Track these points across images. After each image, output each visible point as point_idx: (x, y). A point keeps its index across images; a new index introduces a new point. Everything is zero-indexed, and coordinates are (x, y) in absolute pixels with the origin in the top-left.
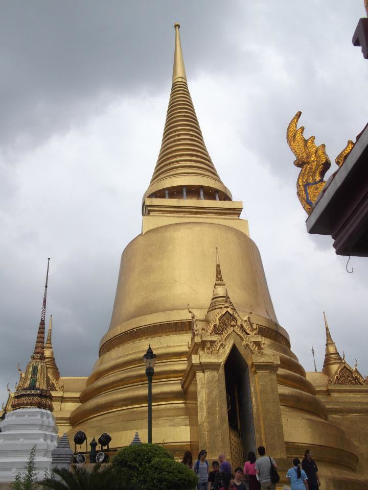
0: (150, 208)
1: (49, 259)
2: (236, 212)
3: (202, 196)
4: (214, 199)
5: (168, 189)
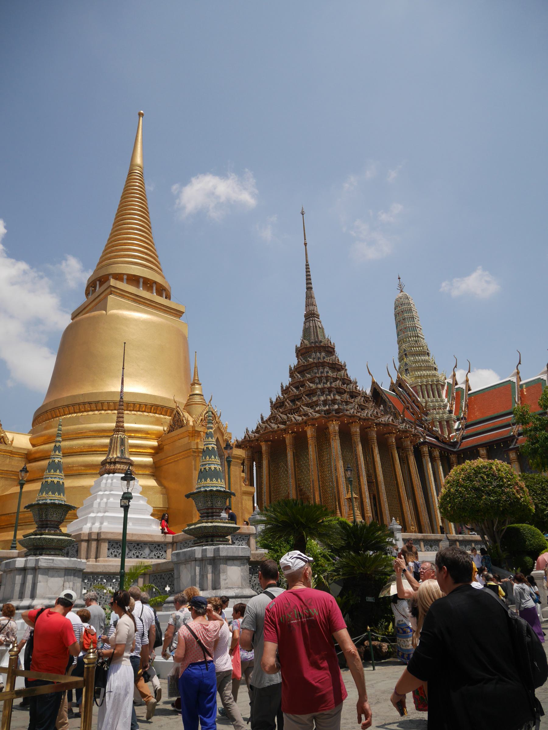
0: (113, 289)
1: (125, 343)
2: (178, 313)
3: (154, 291)
5: (128, 275)
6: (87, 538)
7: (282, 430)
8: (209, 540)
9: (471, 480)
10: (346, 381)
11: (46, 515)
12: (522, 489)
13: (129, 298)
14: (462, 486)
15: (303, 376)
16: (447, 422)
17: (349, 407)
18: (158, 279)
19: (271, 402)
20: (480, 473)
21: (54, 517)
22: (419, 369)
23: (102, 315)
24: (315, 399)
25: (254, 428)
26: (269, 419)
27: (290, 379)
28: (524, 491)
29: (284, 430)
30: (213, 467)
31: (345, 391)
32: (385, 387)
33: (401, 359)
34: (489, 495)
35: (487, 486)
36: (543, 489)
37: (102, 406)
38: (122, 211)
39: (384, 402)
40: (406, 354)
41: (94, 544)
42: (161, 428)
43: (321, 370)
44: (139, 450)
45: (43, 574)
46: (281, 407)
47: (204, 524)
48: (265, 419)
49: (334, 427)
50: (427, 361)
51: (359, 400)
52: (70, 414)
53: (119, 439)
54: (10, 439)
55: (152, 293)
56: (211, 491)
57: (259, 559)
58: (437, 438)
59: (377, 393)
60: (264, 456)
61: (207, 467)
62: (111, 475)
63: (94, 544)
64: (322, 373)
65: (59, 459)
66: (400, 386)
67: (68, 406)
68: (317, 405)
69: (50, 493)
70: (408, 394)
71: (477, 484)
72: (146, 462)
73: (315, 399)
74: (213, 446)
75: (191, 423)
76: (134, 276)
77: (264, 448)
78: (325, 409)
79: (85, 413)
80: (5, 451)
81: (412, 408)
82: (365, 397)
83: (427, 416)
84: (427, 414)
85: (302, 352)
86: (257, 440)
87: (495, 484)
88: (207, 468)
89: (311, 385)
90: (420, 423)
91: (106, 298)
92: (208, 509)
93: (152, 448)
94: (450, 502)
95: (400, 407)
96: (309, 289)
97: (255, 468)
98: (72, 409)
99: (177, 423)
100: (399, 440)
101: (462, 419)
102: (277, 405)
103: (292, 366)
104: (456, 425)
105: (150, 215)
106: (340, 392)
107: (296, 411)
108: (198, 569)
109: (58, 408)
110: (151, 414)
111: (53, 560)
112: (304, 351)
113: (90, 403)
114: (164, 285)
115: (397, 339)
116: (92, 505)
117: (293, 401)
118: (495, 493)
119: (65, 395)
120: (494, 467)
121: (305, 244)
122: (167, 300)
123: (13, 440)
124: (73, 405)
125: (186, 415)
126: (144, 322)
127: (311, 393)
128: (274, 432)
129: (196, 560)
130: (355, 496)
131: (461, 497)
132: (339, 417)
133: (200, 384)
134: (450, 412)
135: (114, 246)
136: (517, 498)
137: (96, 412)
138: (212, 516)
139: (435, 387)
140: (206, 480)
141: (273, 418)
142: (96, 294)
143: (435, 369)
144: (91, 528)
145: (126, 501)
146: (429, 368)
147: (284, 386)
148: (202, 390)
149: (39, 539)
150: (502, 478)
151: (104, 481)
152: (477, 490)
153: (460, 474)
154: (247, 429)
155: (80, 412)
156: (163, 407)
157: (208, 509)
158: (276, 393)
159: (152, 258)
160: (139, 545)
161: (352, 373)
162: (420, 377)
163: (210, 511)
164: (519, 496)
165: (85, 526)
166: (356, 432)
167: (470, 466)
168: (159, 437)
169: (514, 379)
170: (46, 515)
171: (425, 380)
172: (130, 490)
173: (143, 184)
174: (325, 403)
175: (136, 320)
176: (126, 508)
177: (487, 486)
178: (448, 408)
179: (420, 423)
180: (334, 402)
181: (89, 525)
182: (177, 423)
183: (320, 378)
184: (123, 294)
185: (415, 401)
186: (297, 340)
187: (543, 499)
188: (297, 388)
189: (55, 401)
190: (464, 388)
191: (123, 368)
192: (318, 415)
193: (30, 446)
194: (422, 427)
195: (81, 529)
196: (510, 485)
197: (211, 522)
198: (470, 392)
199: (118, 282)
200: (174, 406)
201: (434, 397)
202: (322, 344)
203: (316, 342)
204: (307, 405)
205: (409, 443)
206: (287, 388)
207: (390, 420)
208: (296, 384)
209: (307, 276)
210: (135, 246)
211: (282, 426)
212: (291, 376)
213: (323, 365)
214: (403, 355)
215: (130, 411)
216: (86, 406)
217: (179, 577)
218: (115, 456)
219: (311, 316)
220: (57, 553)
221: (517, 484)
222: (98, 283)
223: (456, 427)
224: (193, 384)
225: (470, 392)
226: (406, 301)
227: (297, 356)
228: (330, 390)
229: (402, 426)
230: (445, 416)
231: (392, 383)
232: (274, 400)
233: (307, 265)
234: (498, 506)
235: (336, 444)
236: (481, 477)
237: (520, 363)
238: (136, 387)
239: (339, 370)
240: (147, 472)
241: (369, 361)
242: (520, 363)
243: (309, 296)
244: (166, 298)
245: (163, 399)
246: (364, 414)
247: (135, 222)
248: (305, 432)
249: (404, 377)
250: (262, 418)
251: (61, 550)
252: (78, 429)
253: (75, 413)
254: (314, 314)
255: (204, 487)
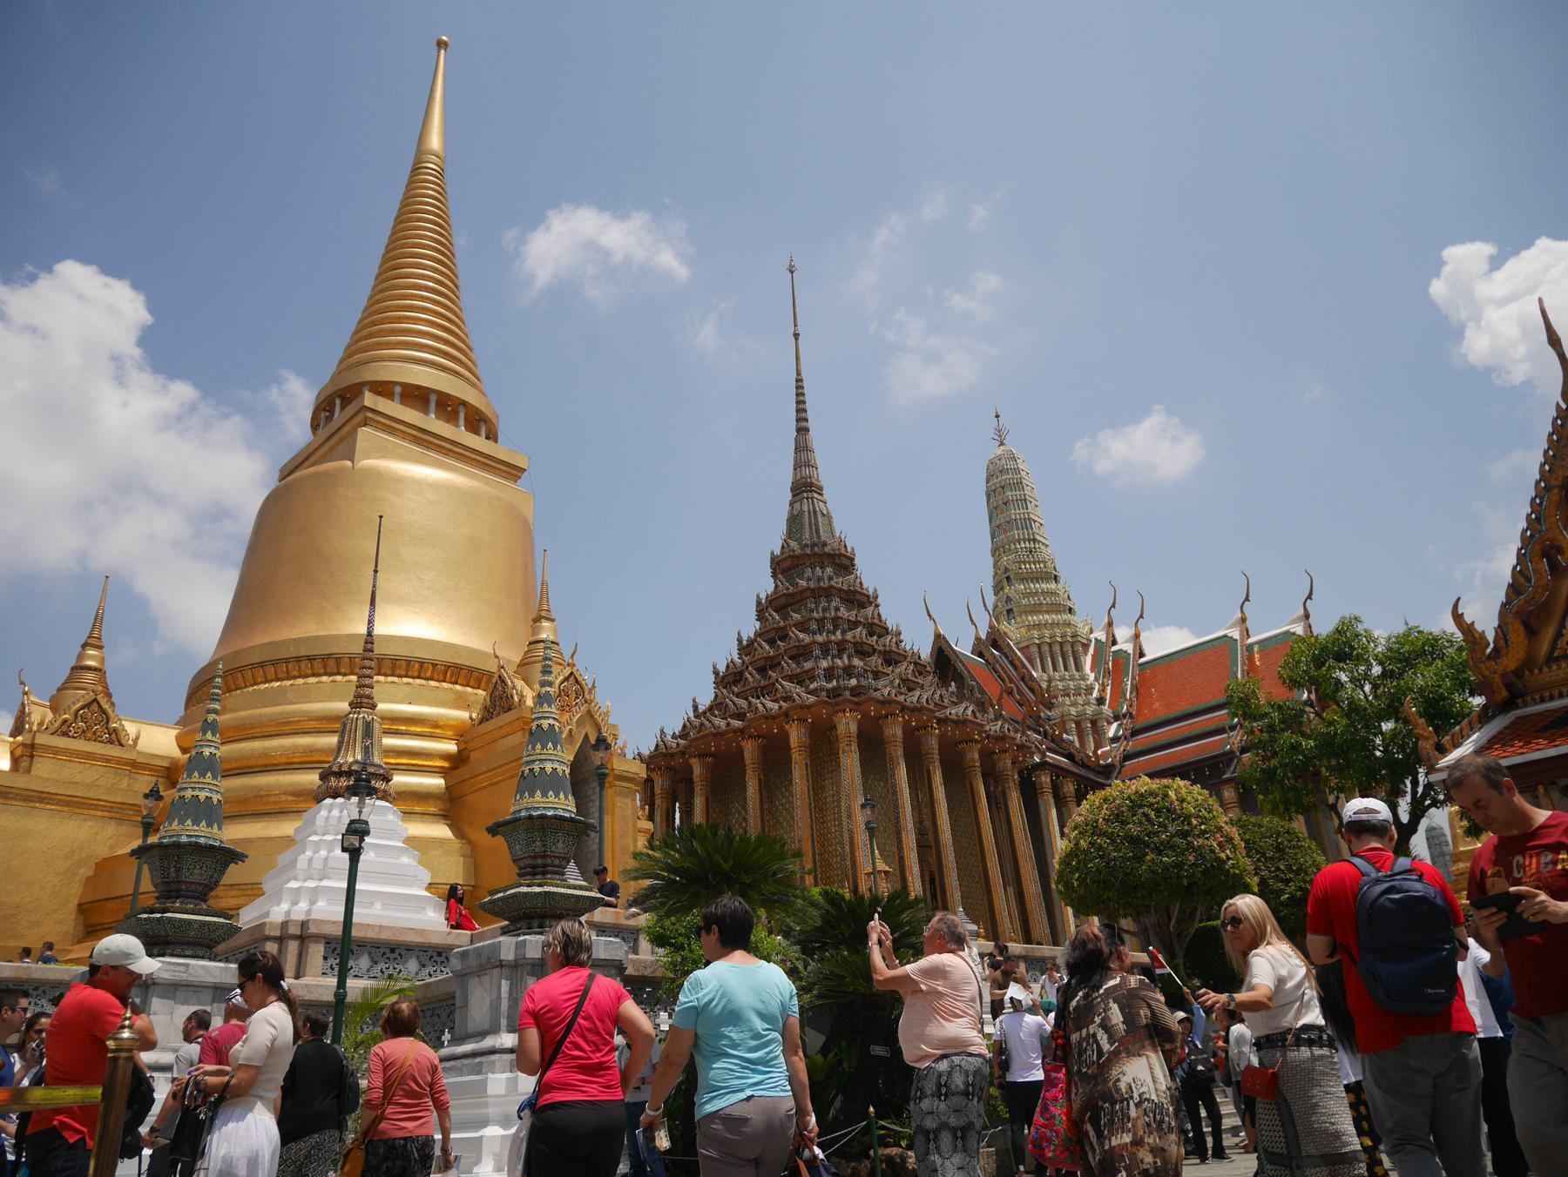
0: (369, 415)
2: (512, 472)
3: (462, 422)
4: (477, 433)
5: (405, 386)
6: (277, 933)
7: (736, 731)
8: (535, 923)
9: (1122, 822)
10: (877, 628)
11: (178, 870)
12: (1230, 840)
13: (404, 436)
14: (1103, 834)
15: (785, 617)
16: (1094, 723)
17: (881, 683)
18: (471, 396)
19: (716, 673)
20: (1141, 806)
21: (195, 874)
22: (1036, 609)
23: (343, 469)
24: (808, 665)
25: (678, 729)
26: (711, 709)
27: (758, 624)
28: (1234, 847)
29: (741, 731)
30: (548, 767)
31: (874, 650)
32: (963, 646)
33: (998, 588)
34: (1160, 853)
35: (1156, 833)
36: (1279, 848)
37: (338, 665)
38: (395, 249)
39: (960, 680)
40: (1008, 578)
41: (293, 947)
42: (465, 715)
43: (824, 604)
44: (415, 761)
45: (163, 997)
46: (735, 683)
47: (525, 889)
48: (701, 708)
49: (847, 724)
50: (1054, 594)
51: (905, 669)
52: (267, 681)
53: (360, 722)
54: (133, 735)
55: (457, 426)
56: (543, 817)
57: (647, 973)
58: (1070, 757)
59: (944, 661)
60: (697, 789)
61: (536, 768)
62: (340, 800)
63: (293, 947)
64: (824, 610)
65: (213, 750)
66: (995, 645)
67: (262, 665)
68: (813, 679)
69: (189, 822)
70: (1011, 663)
71: (1134, 829)
72: (429, 786)
73: (808, 665)
74: (551, 721)
75: (529, 702)
76: (418, 387)
77: (697, 771)
78: (830, 686)
79: (300, 681)
80: (121, 761)
81: (1020, 692)
82: (916, 664)
83: (1050, 709)
84: (1050, 706)
85: (783, 566)
86: (683, 753)
87: (1172, 828)
88: (537, 769)
89: (801, 636)
90: (1036, 723)
91: (354, 432)
92: (535, 857)
93: (446, 756)
94: (1078, 869)
95: (993, 690)
96: (802, 430)
97: (677, 815)
98: (271, 671)
99: (500, 701)
100: (987, 756)
101: (1124, 716)
102: (728, 680)
103: (763, 596)
104: (1112, 731)
105: (457, 260)
106: (862, 651)
107: (768, 690)
108: (505, 985)
109: (241, 669)
110: (445, 685)
111: (187, 965)
112: (788, 564)
113: (311, 659)
114: (483, 409)
115: (989, 545)
116: (294, 862)
117: (762, 671)
118: (1173, 847)
119: (259, 639)
120: (1172, 794)
121: (796, 336)
122: (490, 443)
123: (137, 738)
124: (275, 663)
125: (520, 684)
126: (435, 486)
127: (801, 653)
128: (718, 734)
129: (501, 965)
130: (881, 866)
131: (1101, 857)
132: (858, 704)
133: (552, 620)
134: (1100, 701)
135: (375, 324)
136: (1218, 860)
137: (325, 679)
138: (544, 873)
139: (1069, 649)
140: (532, 795)
141: (717, 706)
142: (333, 426)
143: (1070, 610)
144: (288, 913)
145: (354, 840)
146: (1058, 608)
147: (745, 638)
148: (555, 632)
149: (158, 920)
150: (1188, 818)
151: (324, 813)
152: (1134, 841)
153: (1100, 808)
154: (662, 732)
155: (288, 678)
156: (471, 670)
157: (535, 857)
158: (726, 654)
159: (459, 354)
160: (391, 951)
161: (890, 613)
162: (1038, 626)
163: (539, 861)
164: (1223, 856)
165: (275, 908)
166: (895, 735)
167: (1121, 792)
168: (461, 734)
169: (1236, 635)
170: (178, 870)
171: (1047, 633)
172: (364, 817)
173: (442, 192)
174: (830, 674)
175: (417, 482)
176: (354, 854)
177: (1156, 833)
178: (1095, 694)
179: (1036, 723)
180: (849, 671)
181: (285, 906)
182: (500, 701)
183: (821, 622)
184: (391, 426)
185: (1026, 678)
186: (773, 539)
187: (1278, 869)
188: (771, 642)
189: (236, 654)
190: (1130, 651)
191: (376, 571)
192: (812, 699)
193: (176, 752)
194: (1039, 733)
195: (267, 914)
196: (1205, 832)
197: (540, 885)
198: (1142, 660)
199: (381, 399)
200: (492, 666)
201: (1066, 669)
202: (827, 549)
203: (814, 545)
204: (790, 679)
205: (1009, 763)
206: (751, 642)
207: (969, 712)
208: (770, 634)
209: (798, 403)
210: (423, 326)
211: (737, 723)
212: (761, 616)
213: (828, 593)
214: (1003, 579)
215: (400, 676)
216: (303, 665)
217: (465, 1006)
218: (350, 759)
219: (804, 488)
220: (200, 953)
221: (1220, 829)
222: (338, 402)
223: (1111, 734)
224: (537, 619)
225: (1142, 660)
226: (1011, 465)
227: (774, 576)
228: (841, 647)
229: (995, 728)
230: (1090, 710)
231: (978, 639)
232: (722, 668)
233: (799, 380)
234: (1179, 877)
235: (851, 761)
236: (1144, 814)
237: (1247, 599)
238: (407, 624)
239: (862, 606)
240: (432, 809)
241: (928, 593)
242: (1247, 599)
243: (802, 448)
244: (487, 438)
245: (471, 652)
246: (913, 698)
247: (424, 273)
248: (786, 736)
249: (1004, 627)
250: (695, 707)
251: (210, 947)
252: (281, 713)
253: (278, 679)
254: (811, 485)
255: (527, 809)
